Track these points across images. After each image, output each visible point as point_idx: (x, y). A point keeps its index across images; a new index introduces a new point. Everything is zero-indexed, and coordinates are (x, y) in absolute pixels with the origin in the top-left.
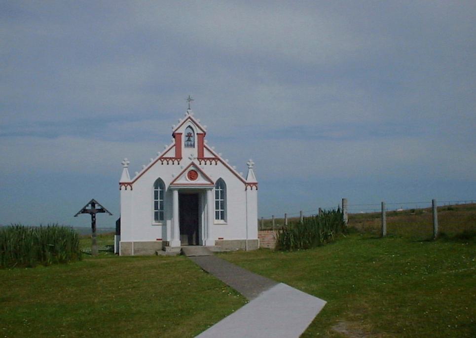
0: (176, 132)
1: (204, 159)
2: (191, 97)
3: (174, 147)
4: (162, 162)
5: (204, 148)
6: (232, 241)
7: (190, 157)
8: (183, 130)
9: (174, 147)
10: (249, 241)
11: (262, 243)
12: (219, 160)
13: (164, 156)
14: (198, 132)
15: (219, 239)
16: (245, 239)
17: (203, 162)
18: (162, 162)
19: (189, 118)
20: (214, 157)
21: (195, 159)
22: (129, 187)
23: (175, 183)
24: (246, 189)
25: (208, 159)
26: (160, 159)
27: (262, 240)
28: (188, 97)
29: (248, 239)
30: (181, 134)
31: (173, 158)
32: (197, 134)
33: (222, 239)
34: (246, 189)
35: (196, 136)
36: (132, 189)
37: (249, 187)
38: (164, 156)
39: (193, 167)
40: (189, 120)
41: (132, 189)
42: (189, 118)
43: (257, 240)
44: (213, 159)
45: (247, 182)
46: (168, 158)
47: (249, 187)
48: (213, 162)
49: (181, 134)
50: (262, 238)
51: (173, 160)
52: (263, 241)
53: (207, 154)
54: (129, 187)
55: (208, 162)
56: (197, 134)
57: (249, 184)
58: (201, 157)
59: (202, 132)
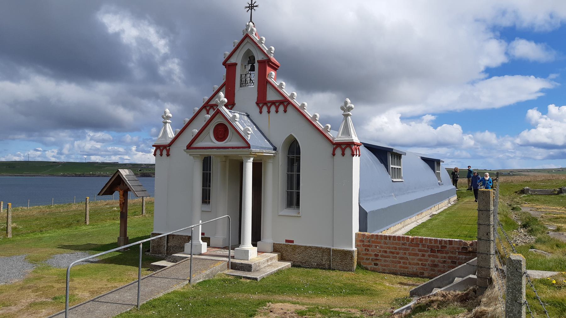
0: (228, 62)
1: (265, 104)
2: (253, 3)
6: (306, 248)
8: (237, 59)
10: (334, 251)
11: (365, 257)
12: (289, 103)
14: (260, 59)
15: (287, 241)
16: (328, 247)
17: (265, 109)
22: (165, 152)
23: (195, 145)
24: (334, 154)
25: (273, 103)
26: (204, 107)
27: (364, 252)
28: (250, 3)
29: (335, 248)
30: (236, 64)
32: (258, 61)
33: (292, 242)
34: (334, 154)
36: (168, 155)
37: (339, 151)
41: (168, 155)
43: (350, 253)
44: (281, 102)
45: (334, 142)
47: (339, 151)
48: (281, 108)
49: (236, 64)
50: (364, 248)
52: (367, 254)
53: (271, 96)
54: (165, 152)
55: (273, 109)
56: (258, 61)
57: (338, 145)
58: (262, 102)
59: (265, 58)
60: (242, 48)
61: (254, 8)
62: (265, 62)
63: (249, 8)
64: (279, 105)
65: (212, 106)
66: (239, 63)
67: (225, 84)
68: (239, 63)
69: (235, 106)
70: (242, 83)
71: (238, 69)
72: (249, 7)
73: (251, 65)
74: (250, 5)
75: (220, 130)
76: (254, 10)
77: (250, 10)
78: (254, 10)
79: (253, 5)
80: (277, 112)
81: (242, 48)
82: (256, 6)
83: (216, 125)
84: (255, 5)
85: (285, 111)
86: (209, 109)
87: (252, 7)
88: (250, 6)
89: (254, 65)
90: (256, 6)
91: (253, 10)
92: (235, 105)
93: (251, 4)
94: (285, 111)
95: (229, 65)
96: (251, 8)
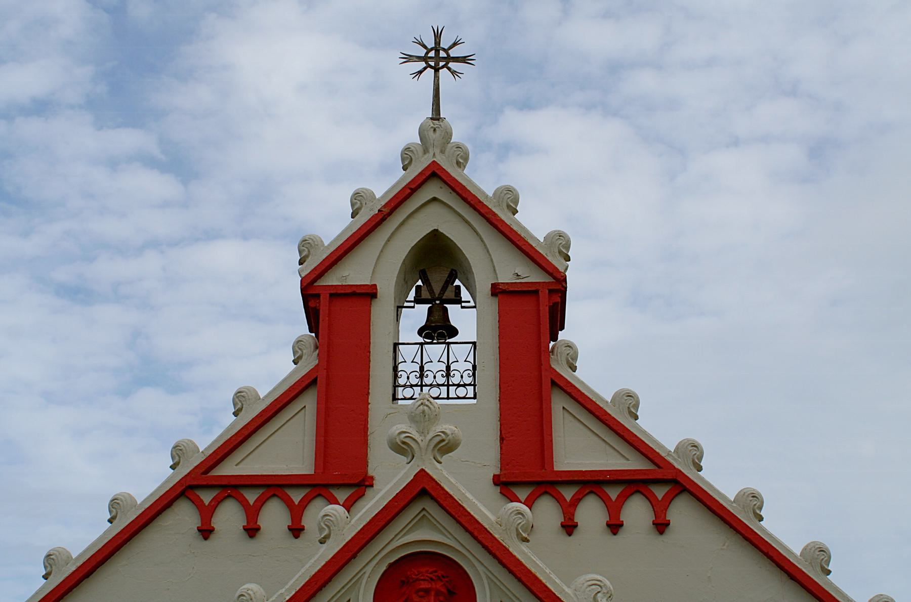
2: (444, 44)
3: (309, 402)
4: (207, 513)
5: (559, 404)
7: (400, 427)
9: (309, 402)
13: (229, 469)
14: (505, 277)
18: (207, 513)
19: (434, 174)
20: (632, 463)
21: (445, 446)
28: (431, 44)
30: (369, 294)
31: (295, 482)
32: (497, 290)
35: (491, 306)
38: (229, 469)
39: (423, 519)
40: (433, 190)
42: (434, 174)
46: (253, 482)
49: (369, 294)
51: (297, 496)
56: (497, 290)
60: (402, 224)
61: (451, 65)
62: (536, 293)
63: (423, 64)
64: (624, 498)
65: (236, 487)
66: (387, 287)
67: (314, 382)
68: (387, 287)
69: (369, 492)
70: (402, 381)
71: (381, 311)
72: (425, 59)
73: (430, 308)
74: (429, 51)
75: (427, 591)
76: (454, 73)
77: (430, 71)
78: (454, 73)
79: (442, 54)
80: (615, 527)
81: (402, 224)
82: (463, 60)
83: (392, 561)
84: (453, 53)
85: (661, 526)
86: (217, 502)
87: (437, 58)
88: (432, 54)
89: (446, 309)
90: (463, 60)
91: (443, 72)
92: (372, 486)
93: (437, 49)
94: (661, 526)
95: (331, 295)
96: (437, 64)
